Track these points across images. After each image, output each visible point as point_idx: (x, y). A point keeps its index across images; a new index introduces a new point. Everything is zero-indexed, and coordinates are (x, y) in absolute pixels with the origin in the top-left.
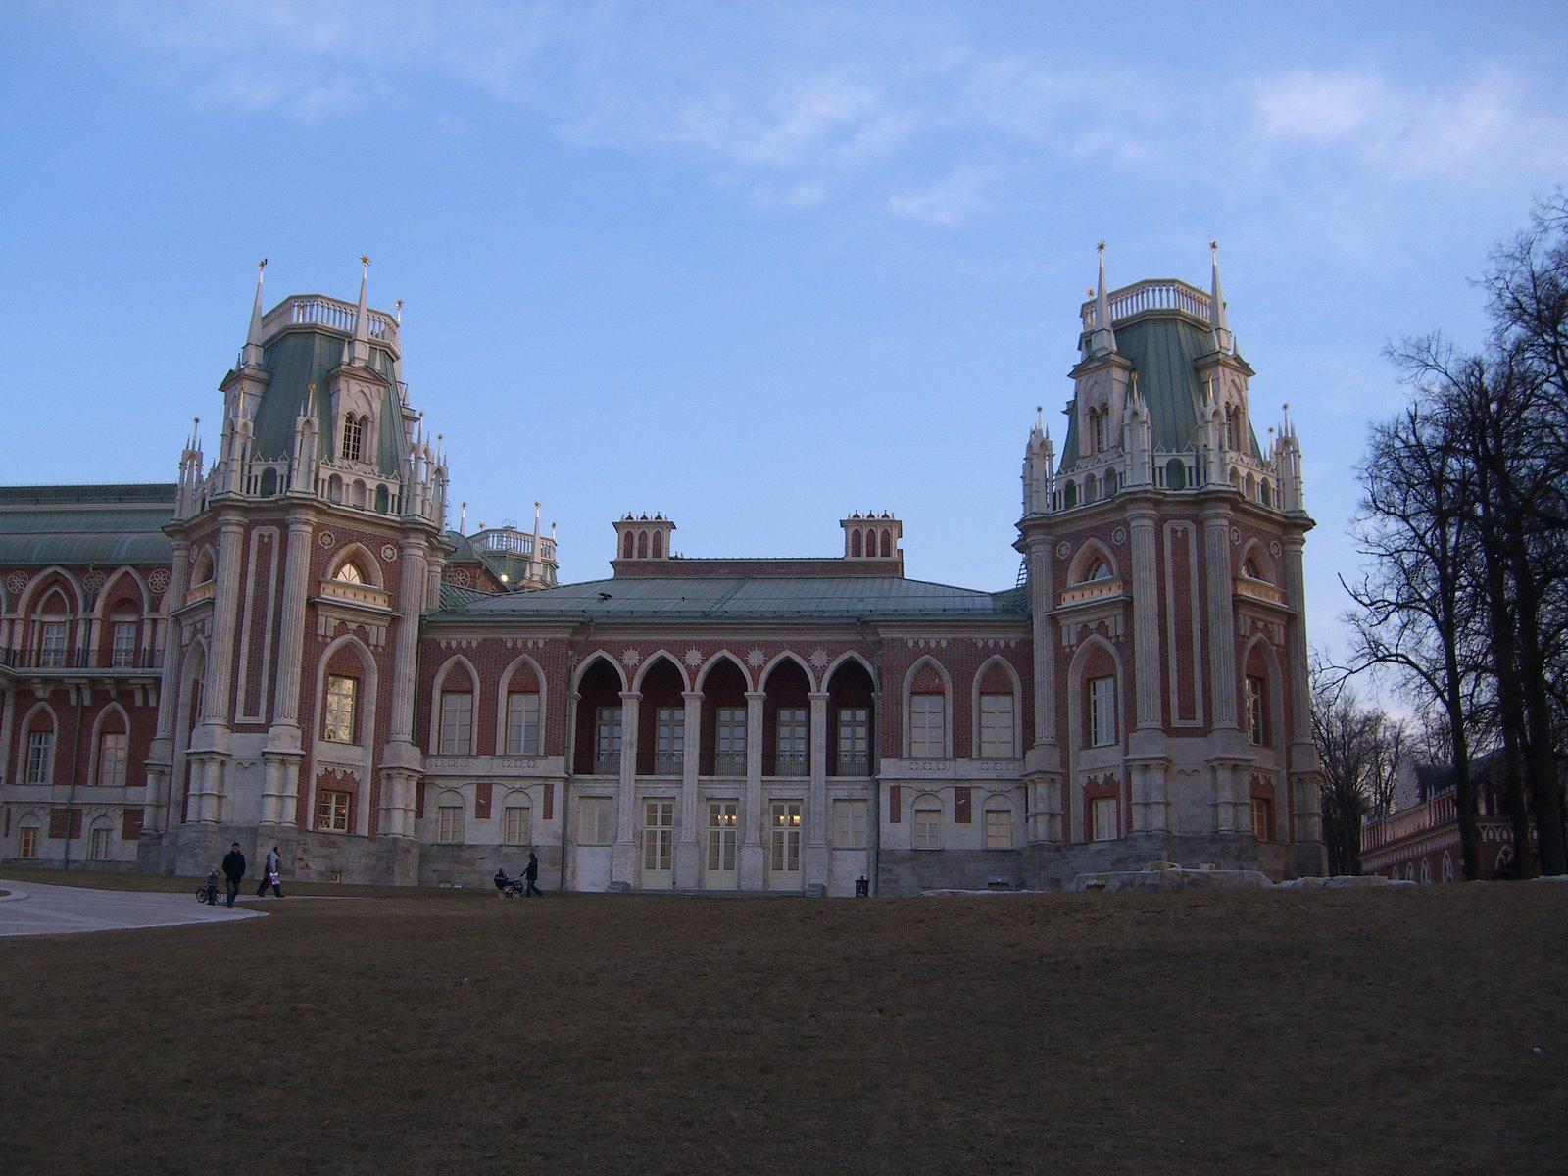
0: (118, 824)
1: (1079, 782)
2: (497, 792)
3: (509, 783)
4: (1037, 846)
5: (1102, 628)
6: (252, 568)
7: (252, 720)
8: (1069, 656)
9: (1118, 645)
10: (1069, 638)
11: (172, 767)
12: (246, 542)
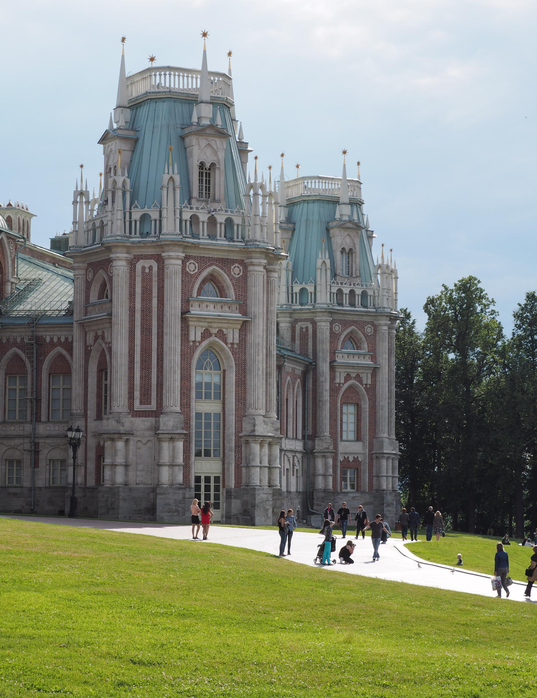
1: (341, 458)
4: (325, 491)
5: (358, 378)
8: (339, 388)
9: (366, 389)
10: (340, 378)
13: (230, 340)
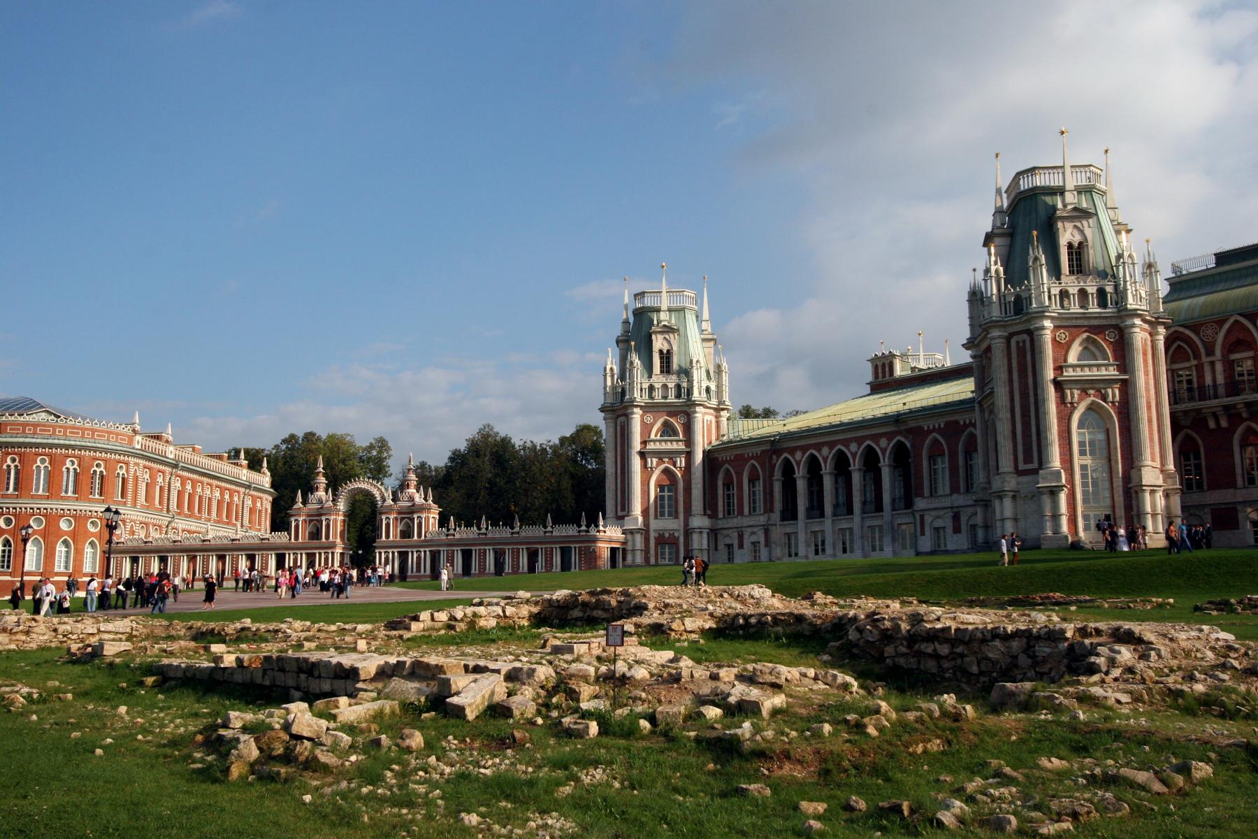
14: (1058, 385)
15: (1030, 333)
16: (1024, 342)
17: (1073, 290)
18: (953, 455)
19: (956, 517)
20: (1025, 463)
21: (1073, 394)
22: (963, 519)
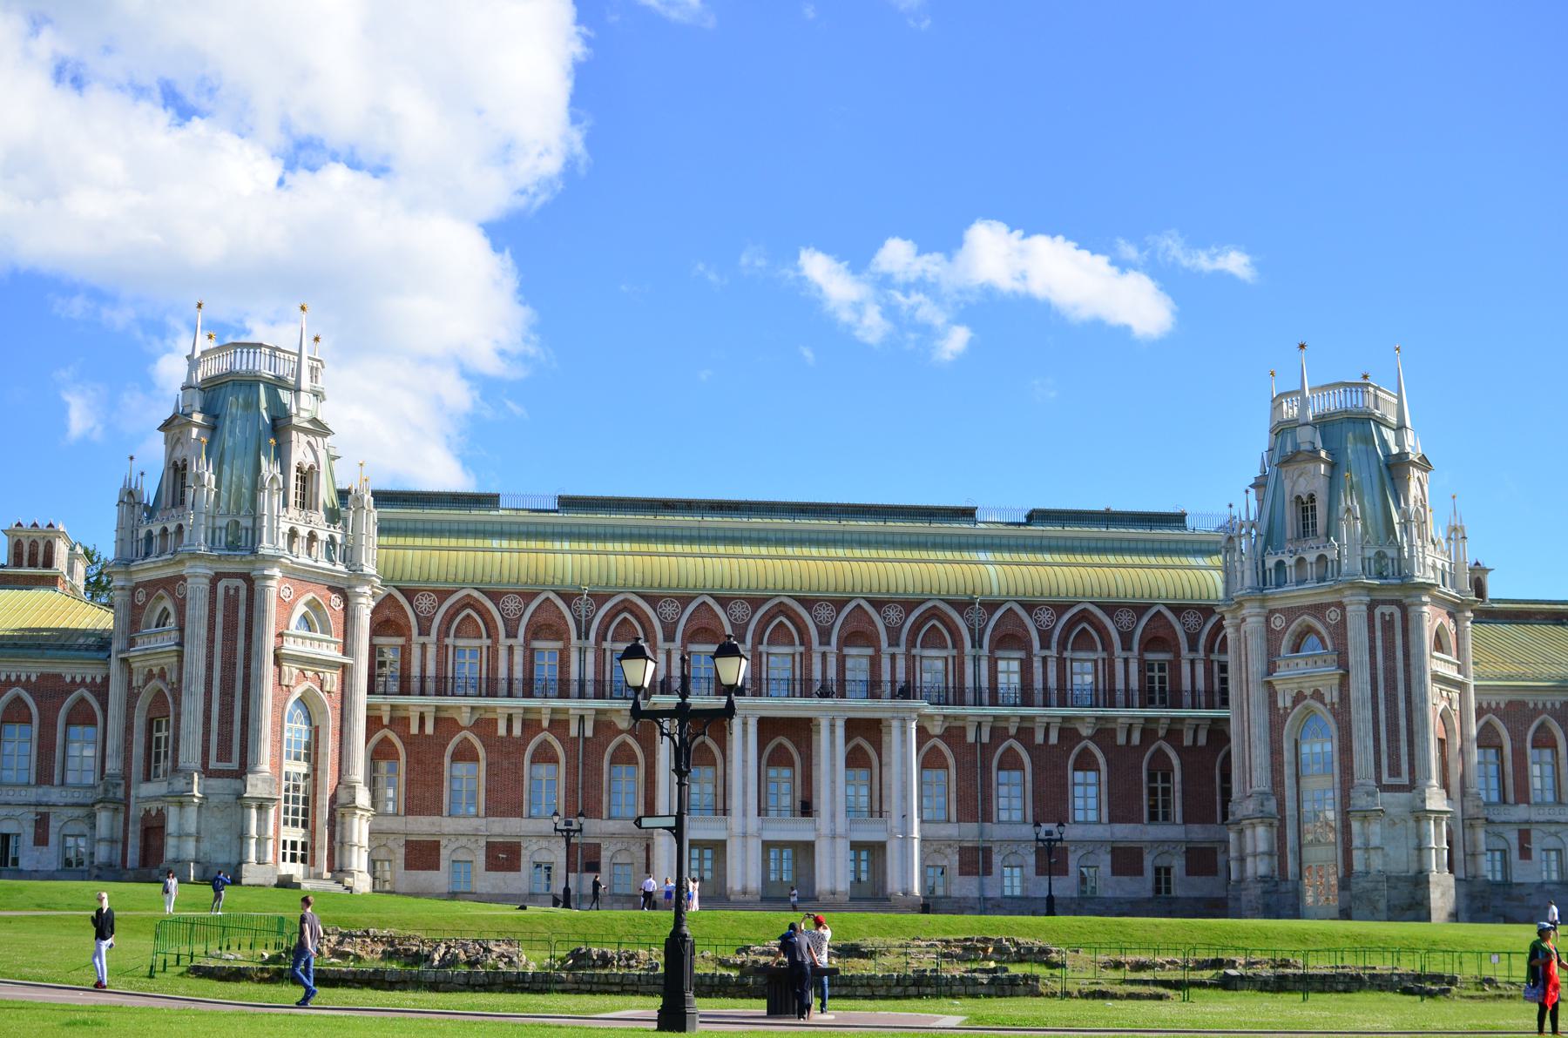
0: (1031, 860)
2: (1535, 834)
3: (1543, 828)
6: (1379, 643)
7: (1394, 781)
11: (1283, 820)
12: (1371, 618)
13: (1327, 700)
14: (278, 660)
15: (248, 579)
16: (237, 589)
17: (303, 531)
18: (47, 727)
19: (42, 823)
20: (219, 760)
21: (291, 670)
22: (54, 825)
